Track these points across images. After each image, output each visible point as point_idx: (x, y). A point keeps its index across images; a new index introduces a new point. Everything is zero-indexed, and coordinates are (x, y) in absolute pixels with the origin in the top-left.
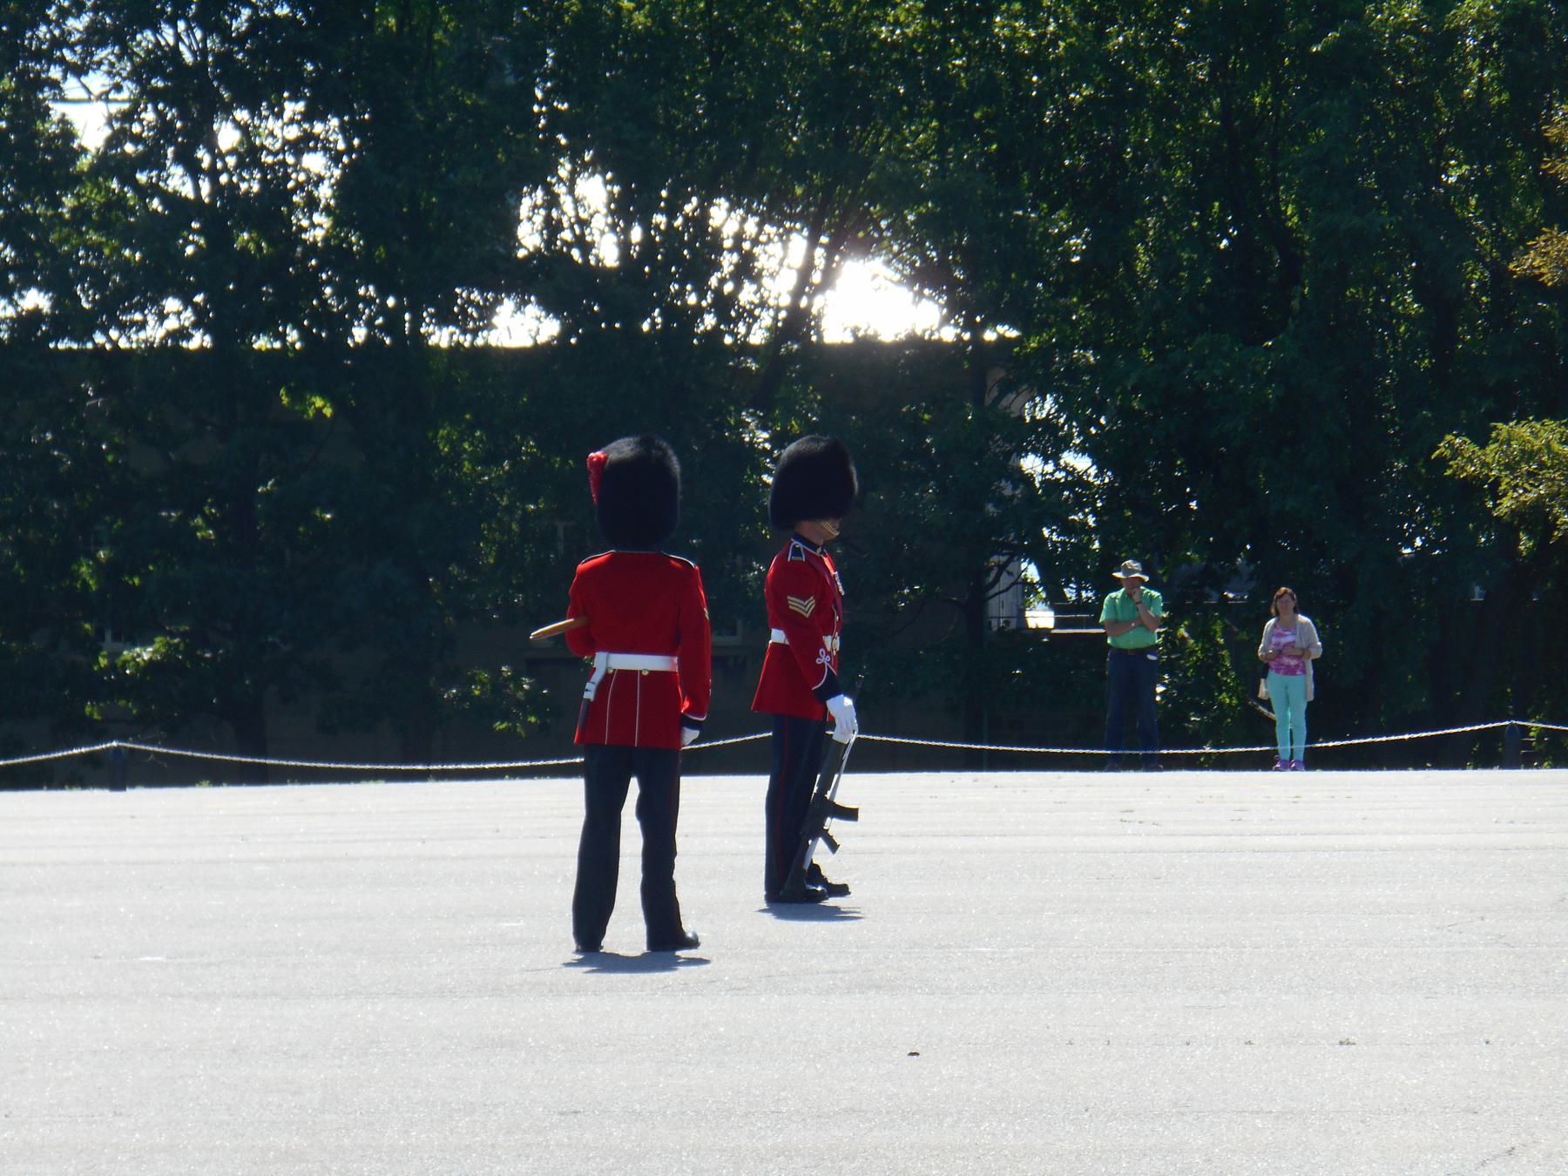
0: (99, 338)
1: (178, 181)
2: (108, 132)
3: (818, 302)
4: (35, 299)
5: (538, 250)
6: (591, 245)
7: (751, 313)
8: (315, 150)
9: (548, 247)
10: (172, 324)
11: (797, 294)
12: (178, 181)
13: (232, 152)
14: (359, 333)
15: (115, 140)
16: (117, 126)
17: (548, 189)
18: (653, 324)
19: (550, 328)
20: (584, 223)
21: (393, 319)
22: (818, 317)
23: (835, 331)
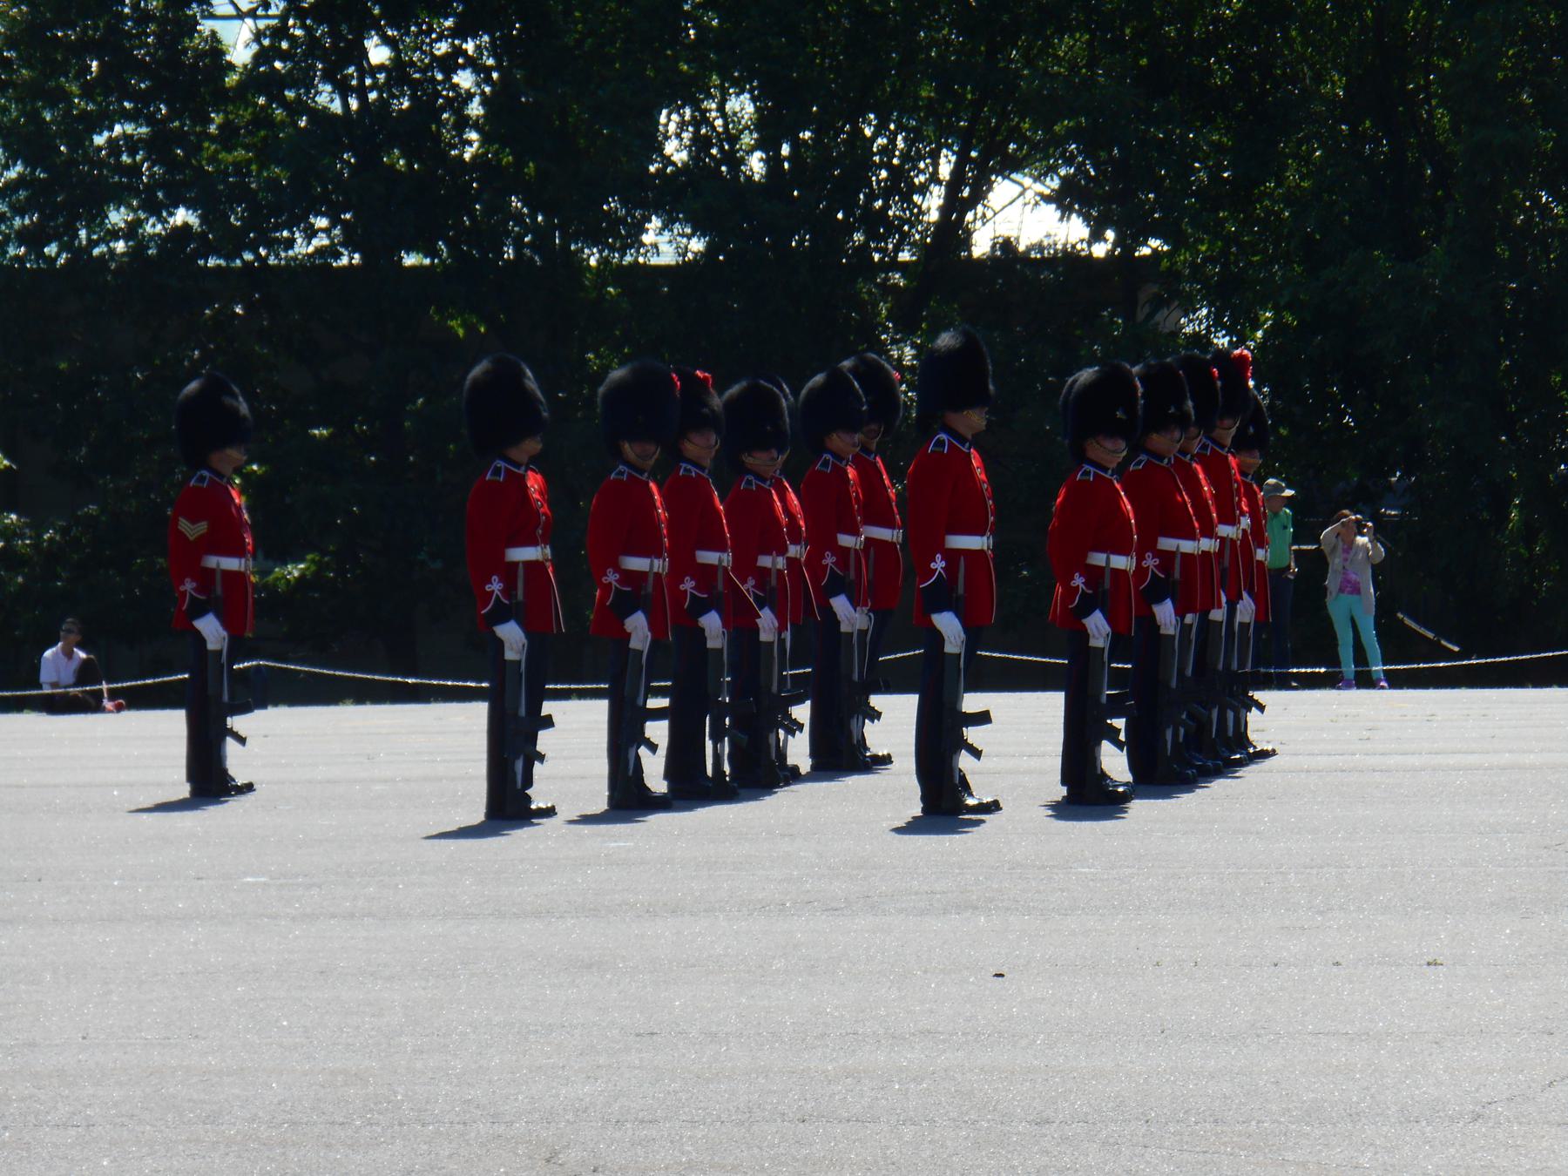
0: (248, 256)
1: (326, 98)
2: (255, 47)
3: (969, 216)
4: (182, 216)
5: (685, 164)
6: (742, 161)
7: (899, 229)
8: (463, 67)
9: (696, 165)
10: (321, 241)
11: (945, 210)
12: (326, 98)
13: (381, 68)
14: (510, 253)
15: (262, 57)
16: (266, 42)
17: (696, 106)
18: (801, 242)
19: (697, 245)
20: (734, 139)
21: (543, 235)
22: (969, 233)
23: (981, 246)
